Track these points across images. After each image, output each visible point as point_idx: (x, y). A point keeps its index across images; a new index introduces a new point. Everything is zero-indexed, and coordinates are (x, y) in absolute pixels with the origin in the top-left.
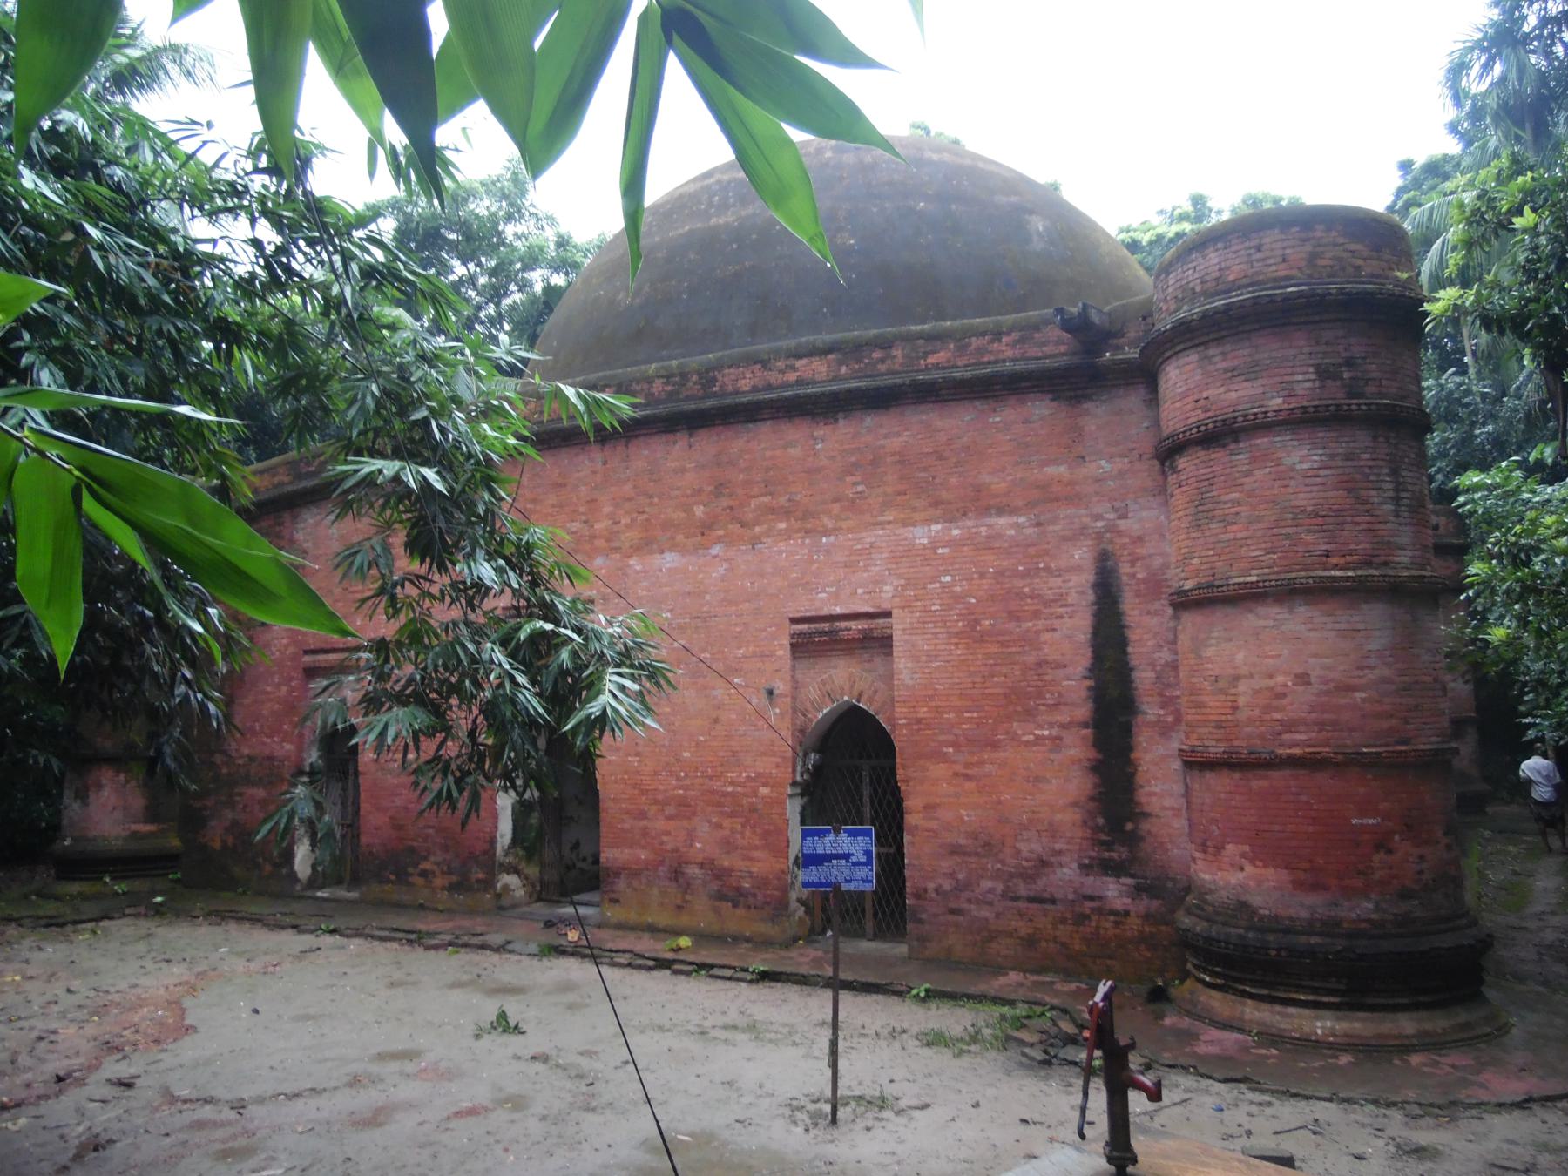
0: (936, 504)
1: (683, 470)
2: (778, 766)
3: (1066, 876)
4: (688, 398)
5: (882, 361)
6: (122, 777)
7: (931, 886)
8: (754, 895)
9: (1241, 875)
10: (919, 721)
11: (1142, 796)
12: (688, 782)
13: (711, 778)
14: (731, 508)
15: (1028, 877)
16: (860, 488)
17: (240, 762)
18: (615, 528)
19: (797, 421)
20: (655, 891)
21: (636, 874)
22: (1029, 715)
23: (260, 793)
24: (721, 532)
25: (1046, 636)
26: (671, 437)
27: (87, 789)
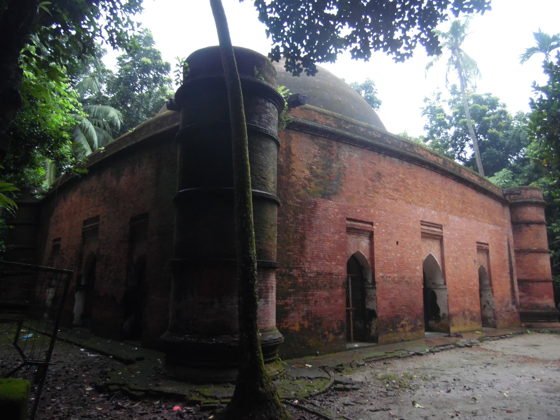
17: (312, 275)
23: (326, 294)
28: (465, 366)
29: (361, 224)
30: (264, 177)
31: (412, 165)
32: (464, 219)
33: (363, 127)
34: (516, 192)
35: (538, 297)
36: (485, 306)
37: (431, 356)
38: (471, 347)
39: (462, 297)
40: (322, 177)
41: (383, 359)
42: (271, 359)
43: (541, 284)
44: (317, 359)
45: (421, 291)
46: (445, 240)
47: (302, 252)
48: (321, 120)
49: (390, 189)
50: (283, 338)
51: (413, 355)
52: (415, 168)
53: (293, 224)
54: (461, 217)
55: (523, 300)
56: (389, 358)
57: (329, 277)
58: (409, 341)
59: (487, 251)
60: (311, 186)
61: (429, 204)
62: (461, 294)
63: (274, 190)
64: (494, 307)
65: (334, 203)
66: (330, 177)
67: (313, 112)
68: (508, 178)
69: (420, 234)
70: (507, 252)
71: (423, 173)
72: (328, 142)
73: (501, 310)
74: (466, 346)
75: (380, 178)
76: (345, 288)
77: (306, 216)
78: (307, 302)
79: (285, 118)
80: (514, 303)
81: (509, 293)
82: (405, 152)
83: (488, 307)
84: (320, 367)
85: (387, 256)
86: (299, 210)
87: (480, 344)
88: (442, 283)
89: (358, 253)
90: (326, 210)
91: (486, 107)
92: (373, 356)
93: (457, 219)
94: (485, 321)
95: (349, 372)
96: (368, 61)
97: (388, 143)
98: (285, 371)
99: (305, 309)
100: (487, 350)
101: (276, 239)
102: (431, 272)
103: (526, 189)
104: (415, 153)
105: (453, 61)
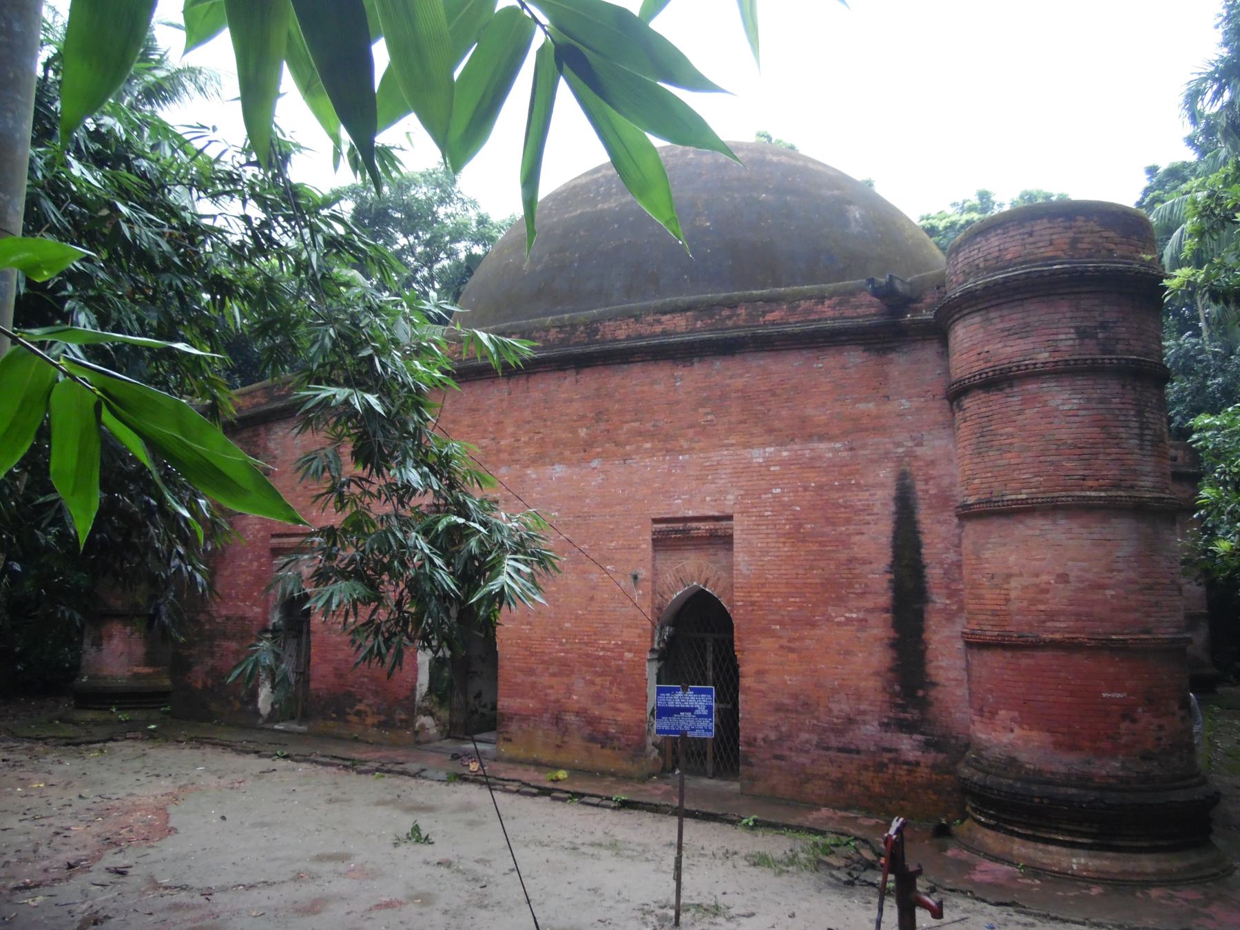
0: (770, 431)
1: (571, 401)
2: (640, 636)
3: (869, 731)
4: (577, 344)
5: (729, 317)
6: (128, 629)
7: (760, 736)
8: (619, 739)
9: (1011, 736)
10: (753, 603)
11: (931, 669)
12: (568, 647)
13: (586, 644)
14: (608, 431)
15: (839, 732)
16: (710, 417)
17: (218, 620)
18: (516, 444)
19: (661, 363)
20: (540, 733)
21: (525, 719)
22: (840, 600)
23: (234, 645)
24: (599, 450)
25: (856, 538)
26: (561, 374)
27: (101, 638)
78: (212, 654)
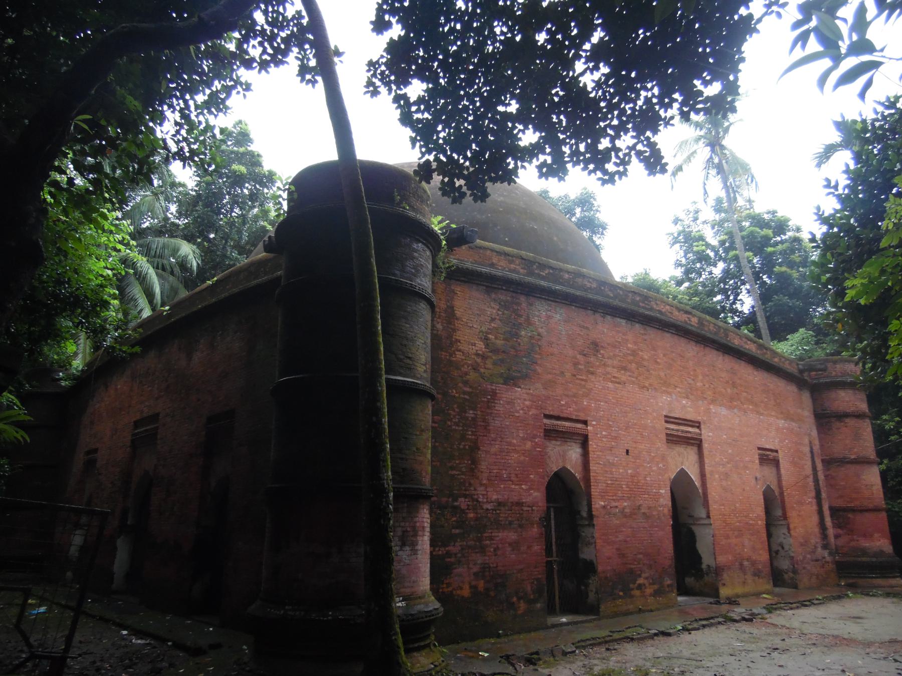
17: (489, 507)
23: (512, 536)
28: (737, 653)
29: (567, 424)
30: (410, 355)
31: (648, 328)
32: (736, 410)
33: (568, 272)
34: (819, 367)
35: (865, 536)
36: (777, 552)
37: (686, 637)
38: (750, 620)
39: (736, 537)
40: (503, 352)
41: (606, 642)
42: (422, 644)
43: (867, 514)
44: (501, 643)
45: (669, 529)
46: (705, 445)
47: (472, 470)
48: (502, 263)
49: (614, 367)
50: (442, 609)
51: (656, 635)
52: (653, 334)
53: (458, 426)
54: (731, 408)
55: (841, 542)
56: (616, 640)
57: (517, 508)
58: (652, 611)
59: (776, 463)
60: (487, 366)
61: (678, 389)
62: (736, 533)
63: (425, 375)
64: (792, 555)
65: (524, 391)
66: (517, 351)
67: (488, 252)
68: (808, 343)
69: (664, 437)
70: (809, 463)
71: (666, 341)
72: (512, 297)
73: (805, 557)
74: (744, 619)
75: (597, 351)
76: (544, 526)
77: (479, 413)
78: (483, 550)
79: (444, 263)
80: (825, 547)
81: (817, 530)
82: (636, 308)
83: (782, 553)
84: (502, 657)
85: (612, 473)
86: (467, 404)
87: (768, 616)
88: (704, 515)
89: (564, 469)
90: (511, 402)
91: (770, 232)
92: (589, 637)
93: (724, 411)
94: (777, 577)
95: (548, 665)
96: (564, 180)
97: (608, 296)
98: (444, 664)
99: (479, 562)
100: (775, 625)
101: (429, 451)
102: (685, 499)
103: (835, 362)
104: (651, 309)
105: (713, 163)
